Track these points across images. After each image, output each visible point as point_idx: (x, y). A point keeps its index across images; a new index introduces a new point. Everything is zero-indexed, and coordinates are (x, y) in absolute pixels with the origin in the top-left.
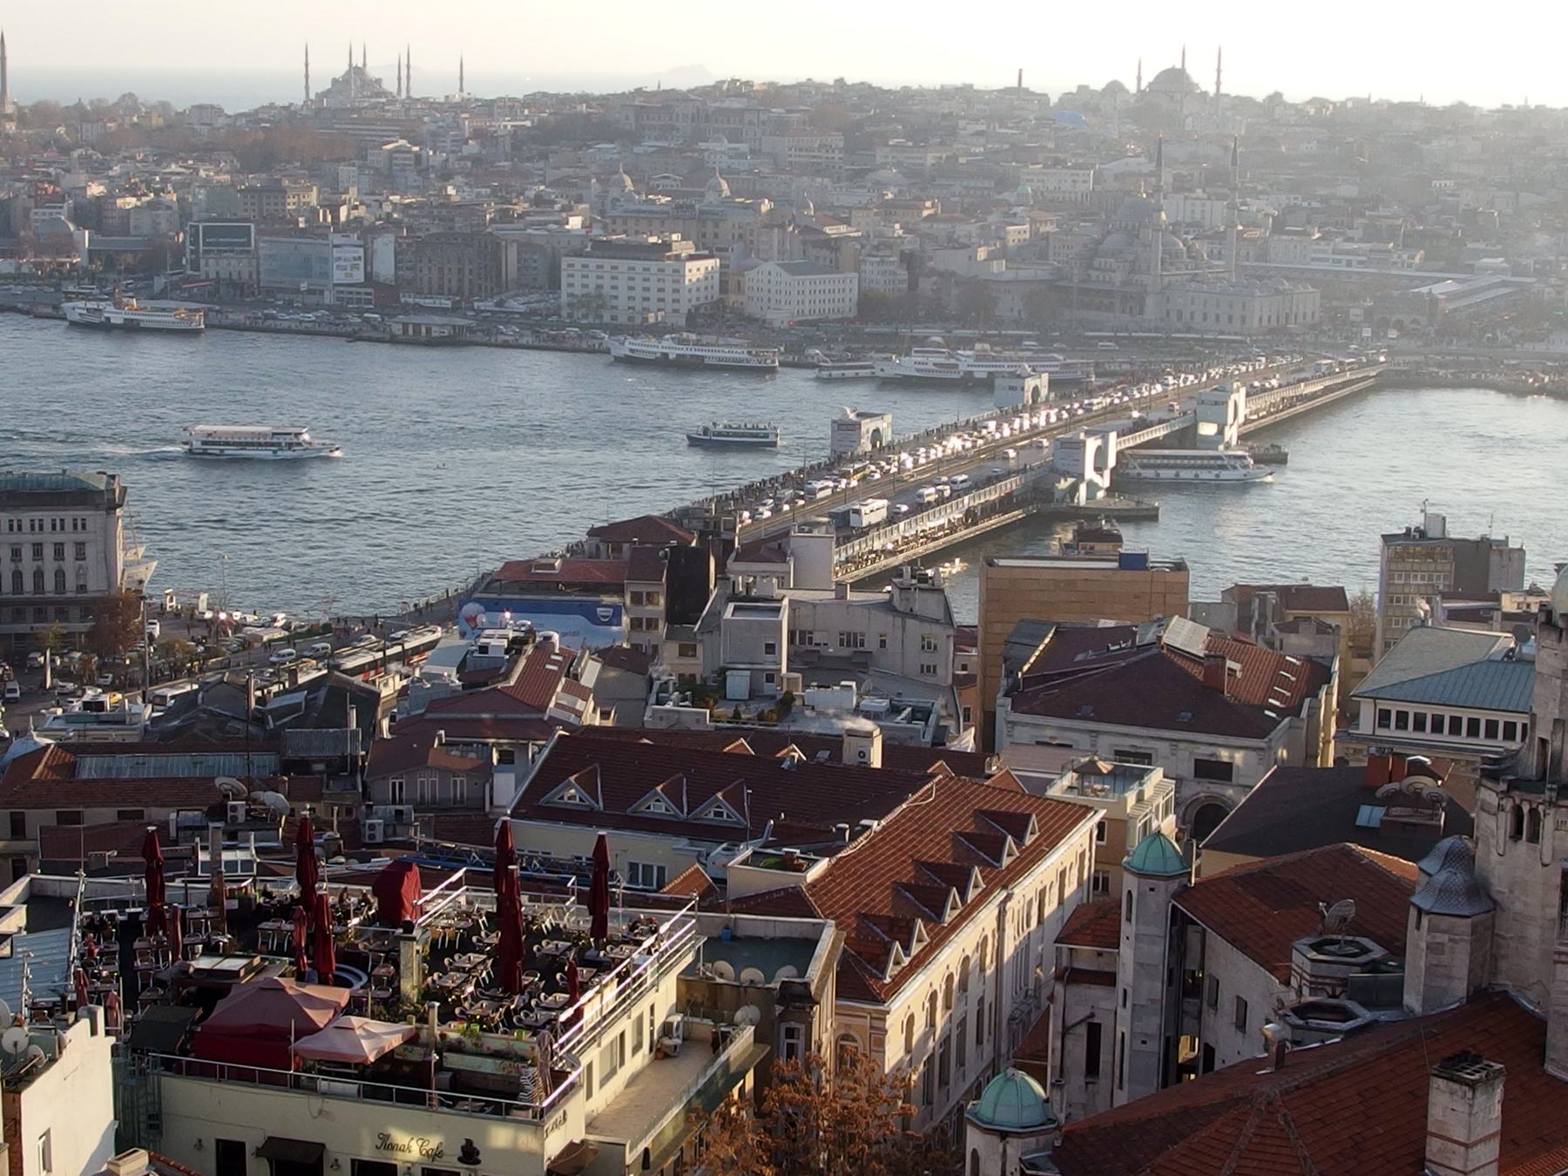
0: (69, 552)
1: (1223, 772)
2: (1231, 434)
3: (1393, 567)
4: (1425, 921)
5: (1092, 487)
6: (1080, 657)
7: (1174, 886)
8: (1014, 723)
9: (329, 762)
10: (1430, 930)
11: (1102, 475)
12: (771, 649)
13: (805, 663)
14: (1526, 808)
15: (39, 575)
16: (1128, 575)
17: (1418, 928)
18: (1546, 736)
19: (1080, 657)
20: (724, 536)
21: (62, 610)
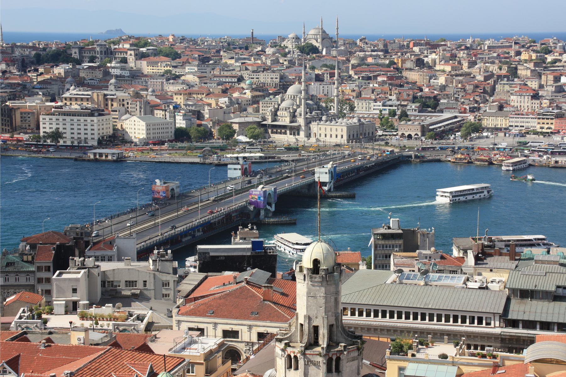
5: (267, 211)
6: (212, 289)
11: (271, 207)
12: (75, 291)
13: (110, 295)
14: (292, 355)
18: (303, 323)
20: (85, 239)
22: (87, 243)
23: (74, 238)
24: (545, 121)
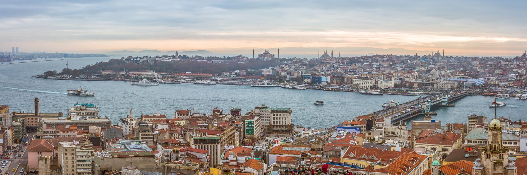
0: (284, 119)
1: (445, 150)
2: (446, 103)
3: (469, 120)
4: (475, 170)
5: (427, 110)
6: (426, 135)
7: (439, 167)
8: (416, 144)
9: (318, 149)
10: (475, 172)
14: (488, 154)
15: (280, 122)
16: (432, 123)
17: (474, 171)
19: (426, 135)
21: (283, 126)
22: (375, 119)
23: (372, 118)
24: (510, 83)
